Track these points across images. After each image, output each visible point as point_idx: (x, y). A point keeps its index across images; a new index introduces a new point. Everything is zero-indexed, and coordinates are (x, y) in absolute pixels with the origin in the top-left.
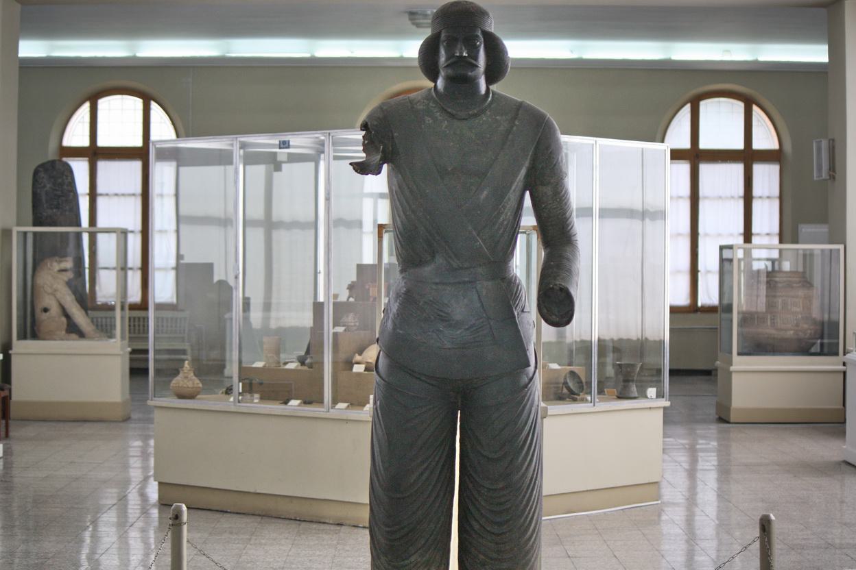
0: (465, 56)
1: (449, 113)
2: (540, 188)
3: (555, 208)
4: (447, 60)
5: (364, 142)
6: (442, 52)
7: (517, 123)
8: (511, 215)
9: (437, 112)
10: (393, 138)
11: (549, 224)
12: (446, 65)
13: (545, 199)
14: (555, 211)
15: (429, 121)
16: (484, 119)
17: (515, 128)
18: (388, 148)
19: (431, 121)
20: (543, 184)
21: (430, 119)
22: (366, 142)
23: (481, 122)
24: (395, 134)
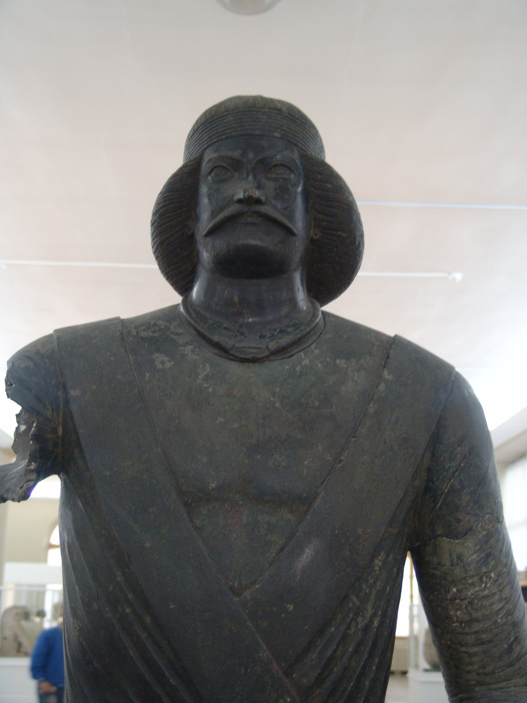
0: (258, 201)
1: (218, 346)
2: (445, 543)
3: (487, 596)
4: (213, 214)
5: (18, 429)
6: (204, 201)
7: (386, 375)
8: (374, 615)
9: (187, 344)
10: (67, 402)
11: (470, 639)
12: (211, 225)
13: (458, 571)
14: (486, 603)
15: (163, 363)
16: (306, 362)
17: (382, 387)
18: (54, 430)
19: (168, 365)
20: (453, 535)
21: (166, 359)
22: (23, 428)
23: (298, 368)
24: (74, 393)
